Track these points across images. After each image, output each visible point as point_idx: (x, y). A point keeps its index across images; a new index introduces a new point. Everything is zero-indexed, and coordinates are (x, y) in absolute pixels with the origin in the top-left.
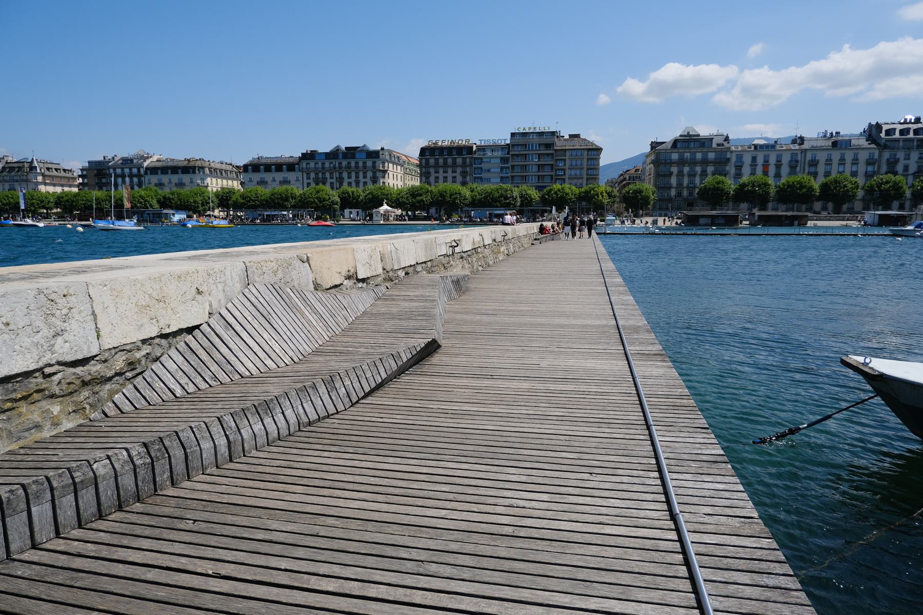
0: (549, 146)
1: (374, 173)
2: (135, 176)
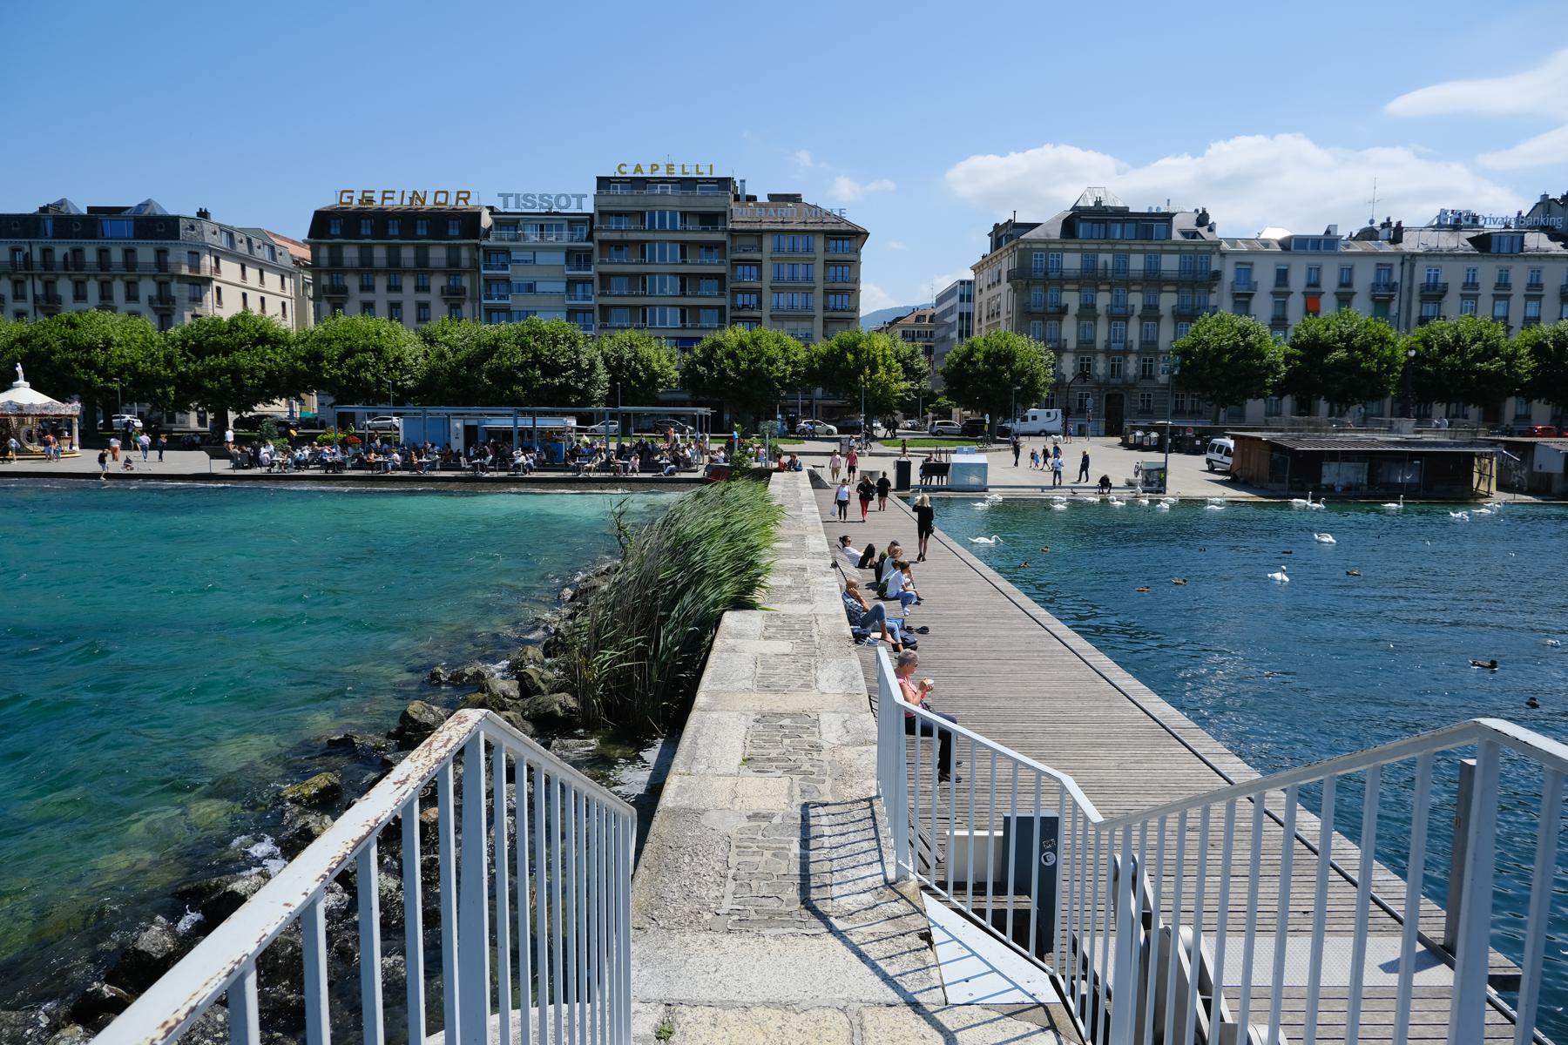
0: (711, 219)
1: (163, 285)
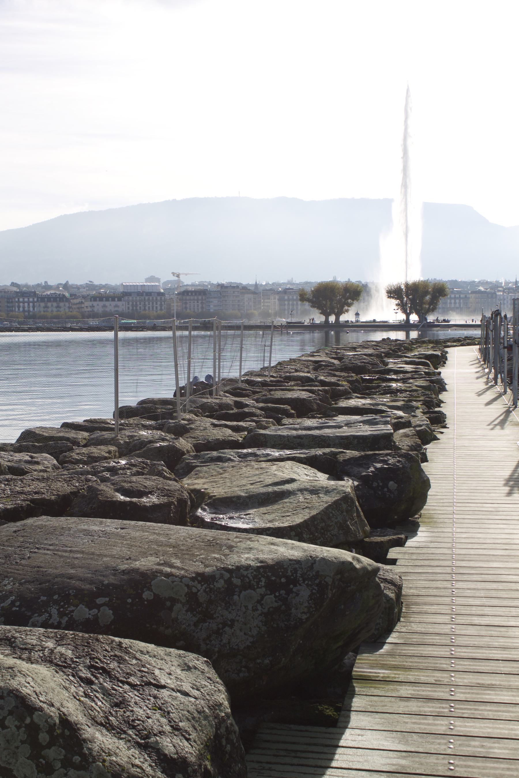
2: (31, 302)
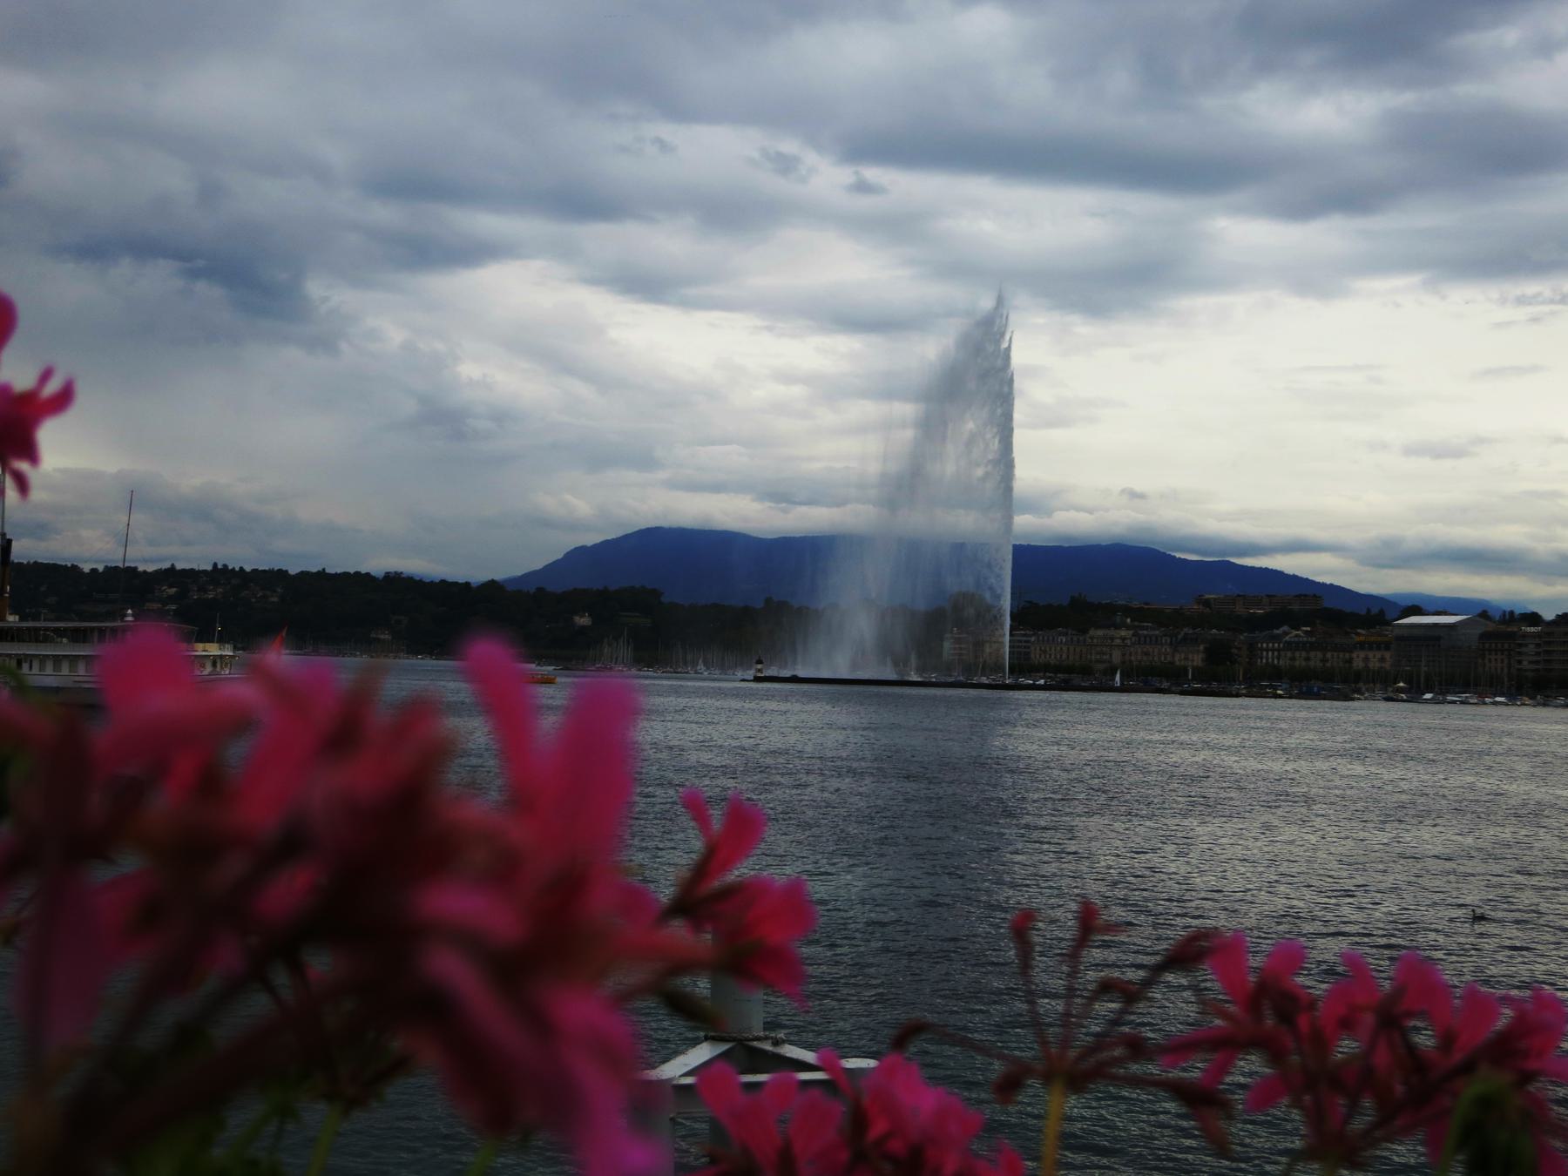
2: (1276, 650)
